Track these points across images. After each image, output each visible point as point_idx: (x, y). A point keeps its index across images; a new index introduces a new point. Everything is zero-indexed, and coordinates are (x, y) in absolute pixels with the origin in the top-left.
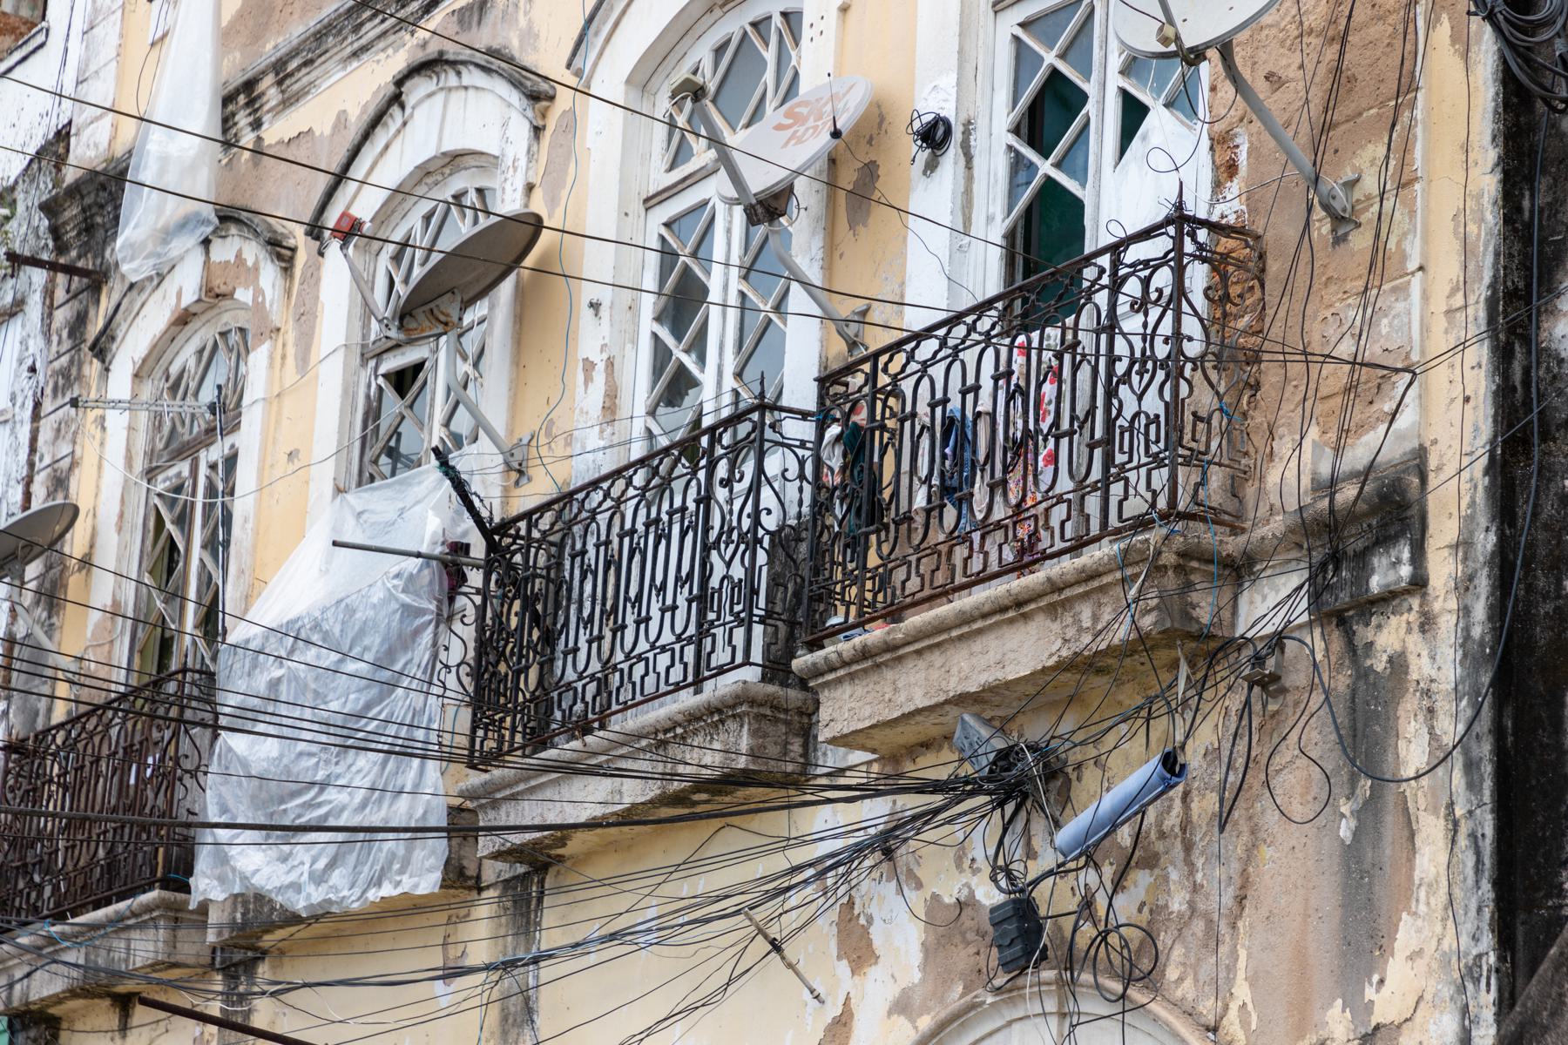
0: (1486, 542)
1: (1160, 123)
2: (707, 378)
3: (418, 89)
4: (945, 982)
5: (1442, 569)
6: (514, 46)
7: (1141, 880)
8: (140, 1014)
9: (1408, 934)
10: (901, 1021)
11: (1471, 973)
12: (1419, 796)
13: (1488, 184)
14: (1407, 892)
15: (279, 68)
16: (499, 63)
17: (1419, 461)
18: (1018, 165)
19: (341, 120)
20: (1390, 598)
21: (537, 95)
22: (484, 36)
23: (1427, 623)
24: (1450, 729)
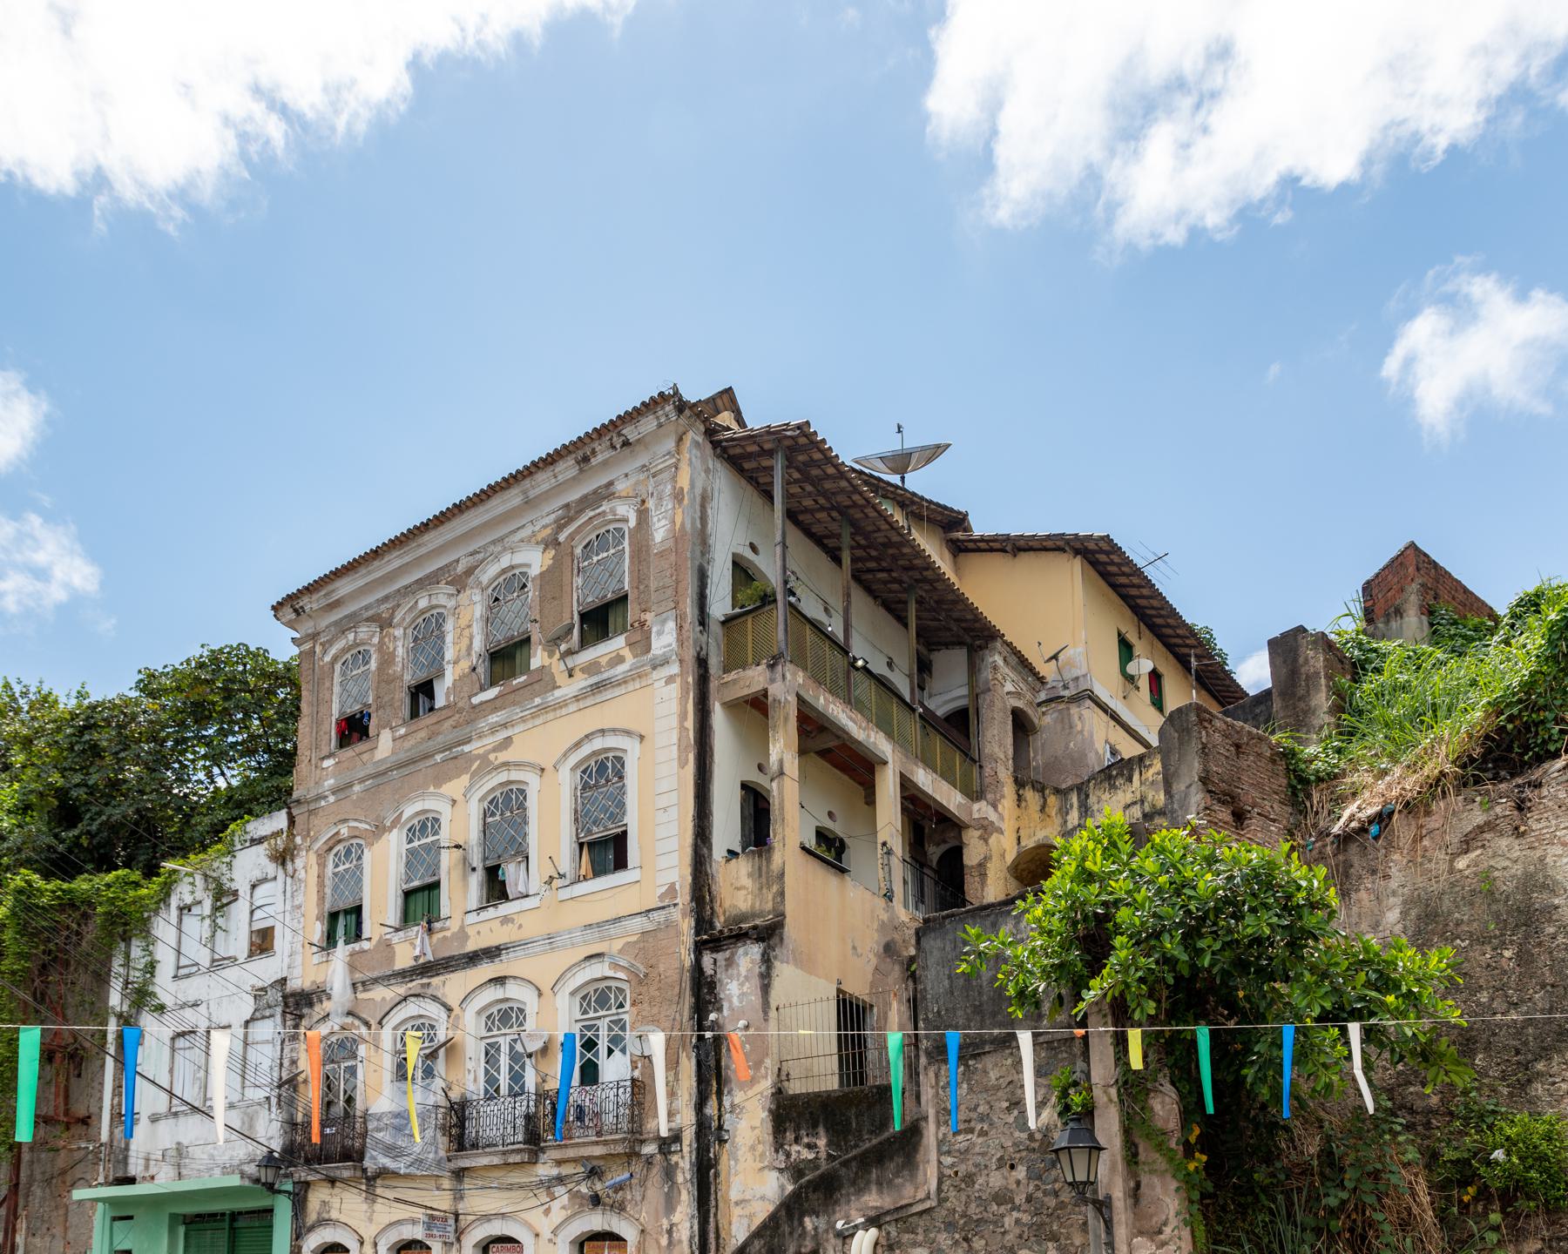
0: (695, 1146)
1: (617, 1053)
2: (501, 1078)
3: (412, 999)
4: (574, 1205)
5: (686, 1149)
6: (440, 996)
7: (621, 1193)
8: (338, 1184)
9: (679, 1209)
10: (564, 1211)
11: (693, 1217)
12: (681, 1187)
13: (695, 1084)
14: (679, 1202)
15: (363, 983)
16: (435, 998)
17: (681, 1130)
18: (581, 1053)
19: (384, 999)
20: (675, 1152)
21: (450, 1010)
22: (430, 991)
23: (683, 1157)
24: (688, 1177)
